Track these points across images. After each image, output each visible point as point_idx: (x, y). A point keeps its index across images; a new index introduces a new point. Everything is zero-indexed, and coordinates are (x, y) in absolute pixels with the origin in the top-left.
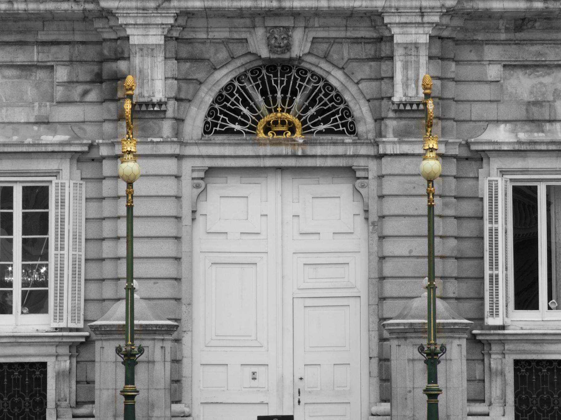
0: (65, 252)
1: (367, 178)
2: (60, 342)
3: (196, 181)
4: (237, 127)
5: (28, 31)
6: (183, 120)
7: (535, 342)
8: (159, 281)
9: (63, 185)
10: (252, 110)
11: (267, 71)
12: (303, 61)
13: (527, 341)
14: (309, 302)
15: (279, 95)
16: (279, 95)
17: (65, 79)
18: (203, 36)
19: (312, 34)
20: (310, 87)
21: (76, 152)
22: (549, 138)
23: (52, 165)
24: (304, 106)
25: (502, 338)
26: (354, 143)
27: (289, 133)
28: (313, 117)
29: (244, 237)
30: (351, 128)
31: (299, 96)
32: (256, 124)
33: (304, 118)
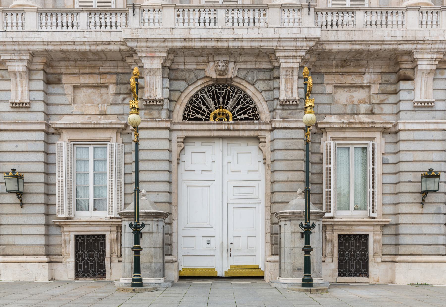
0: (114, 179)
1: (265, 142)
2: (111, 225)
3: (179, 144)
4: (200, 116)
5: (95, 67)
6: (173, 112)
7: (349, 225)
8: (160, 193)
9: (112, 145)
10: (207, 108)
11: (215, 88)
12: (233, 81)
13: (345, 225)
14: (235, 206)
15: (221, 100)
16: (221, 100)
17: (114, 92)
18: (182, 67)
19: (238, 66)
20: (237, 96)
21: (119, 128)
22: (357, 121)
23: (107, 135)
24: (234, 106)
25: (332, 223)
26: (260, 123)
27: (226, 120)
28: (238, 111)
29: (203, 172)
30: (257, 117)
31: (231, 100)
32: (209, 115)
33: (234, 112)
